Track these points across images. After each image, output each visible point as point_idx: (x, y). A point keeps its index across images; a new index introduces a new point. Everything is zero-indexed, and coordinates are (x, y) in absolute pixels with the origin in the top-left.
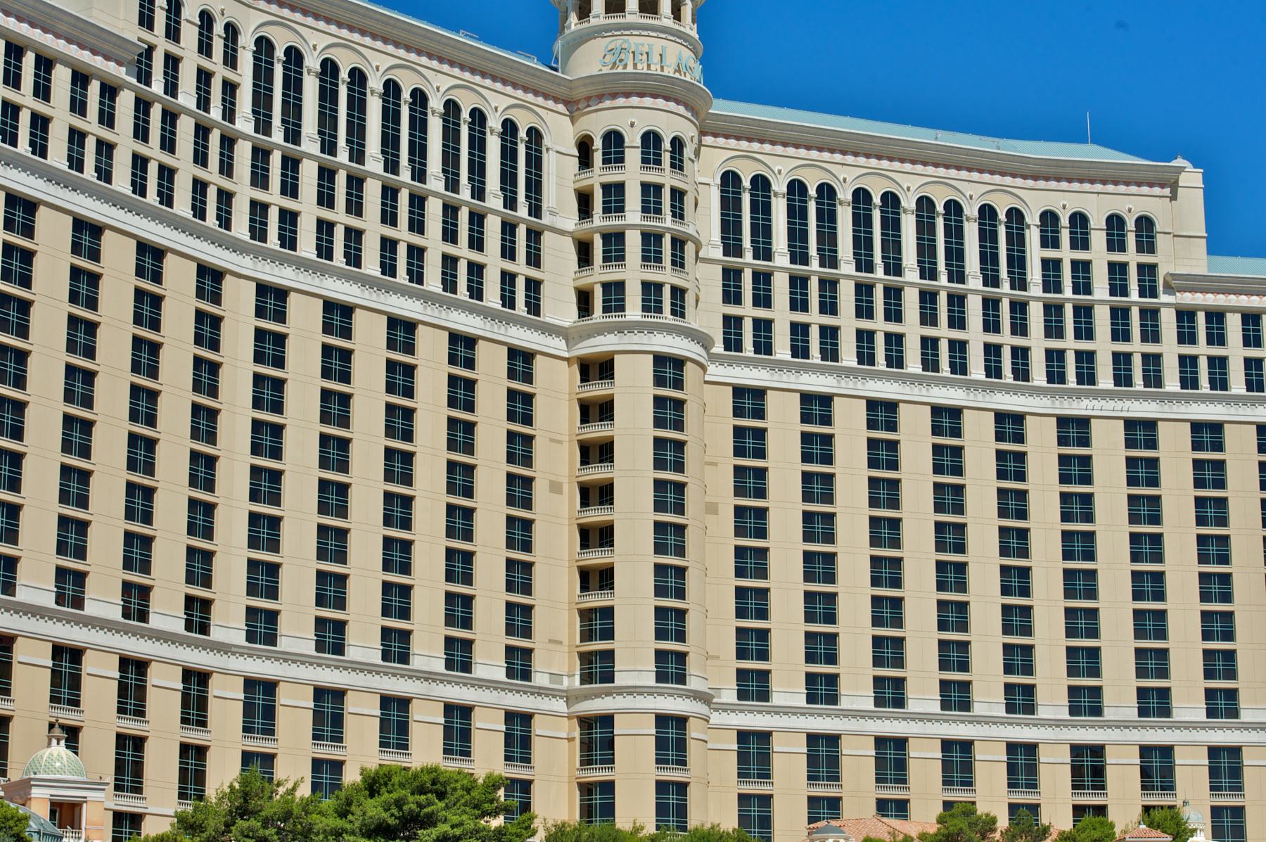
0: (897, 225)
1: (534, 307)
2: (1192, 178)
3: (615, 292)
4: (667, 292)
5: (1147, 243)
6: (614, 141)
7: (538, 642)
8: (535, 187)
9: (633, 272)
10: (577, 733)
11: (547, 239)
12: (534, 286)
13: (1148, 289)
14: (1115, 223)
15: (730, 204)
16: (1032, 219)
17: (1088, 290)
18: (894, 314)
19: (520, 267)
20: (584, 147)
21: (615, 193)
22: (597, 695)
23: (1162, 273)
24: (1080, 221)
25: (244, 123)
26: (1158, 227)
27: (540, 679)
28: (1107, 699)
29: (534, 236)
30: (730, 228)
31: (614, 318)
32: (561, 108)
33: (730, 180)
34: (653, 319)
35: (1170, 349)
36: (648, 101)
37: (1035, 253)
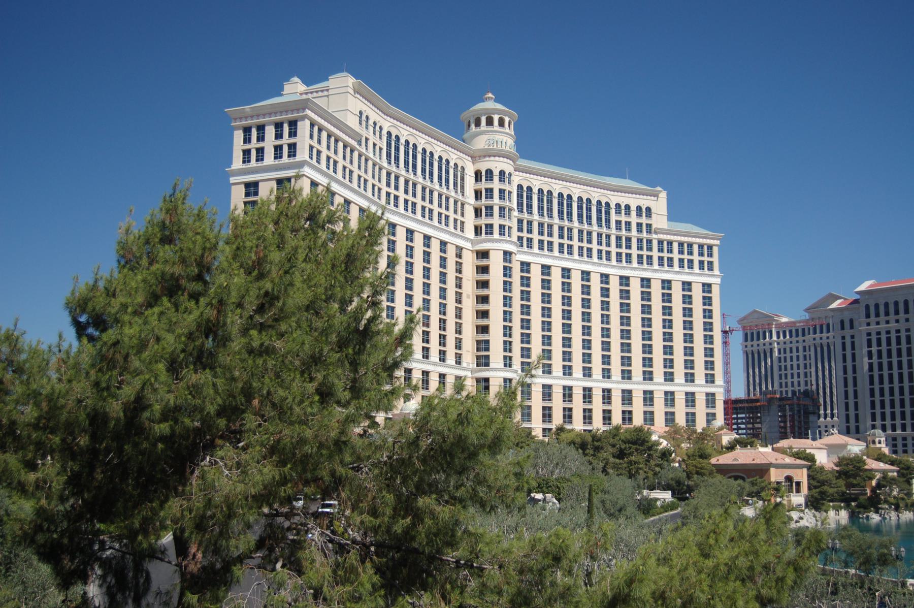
0: (590, 210)
1: (462, 231)
2: (663, 195)
3: (489, 227)
4: (507, 228)
6: (489, 172)
7: (463, 352)
8: (463, 187)
9: (496, 221)
11: (466, 206)
12: (462, 223)
14: (639, 209)
15: (520, 196)
16: (613, 206)
19: (459, 217)
21: (489, 192)
22: (484, 371)
23: (654, 227)
24: (628, 207)
27: (464, 364)
28: (633, 374)
30: (520, 205)
31: (489, 237)
32: (470, 159)
33: (520, 187)
34: (502, 238)
36: (501, 159)
37: (614, 217)
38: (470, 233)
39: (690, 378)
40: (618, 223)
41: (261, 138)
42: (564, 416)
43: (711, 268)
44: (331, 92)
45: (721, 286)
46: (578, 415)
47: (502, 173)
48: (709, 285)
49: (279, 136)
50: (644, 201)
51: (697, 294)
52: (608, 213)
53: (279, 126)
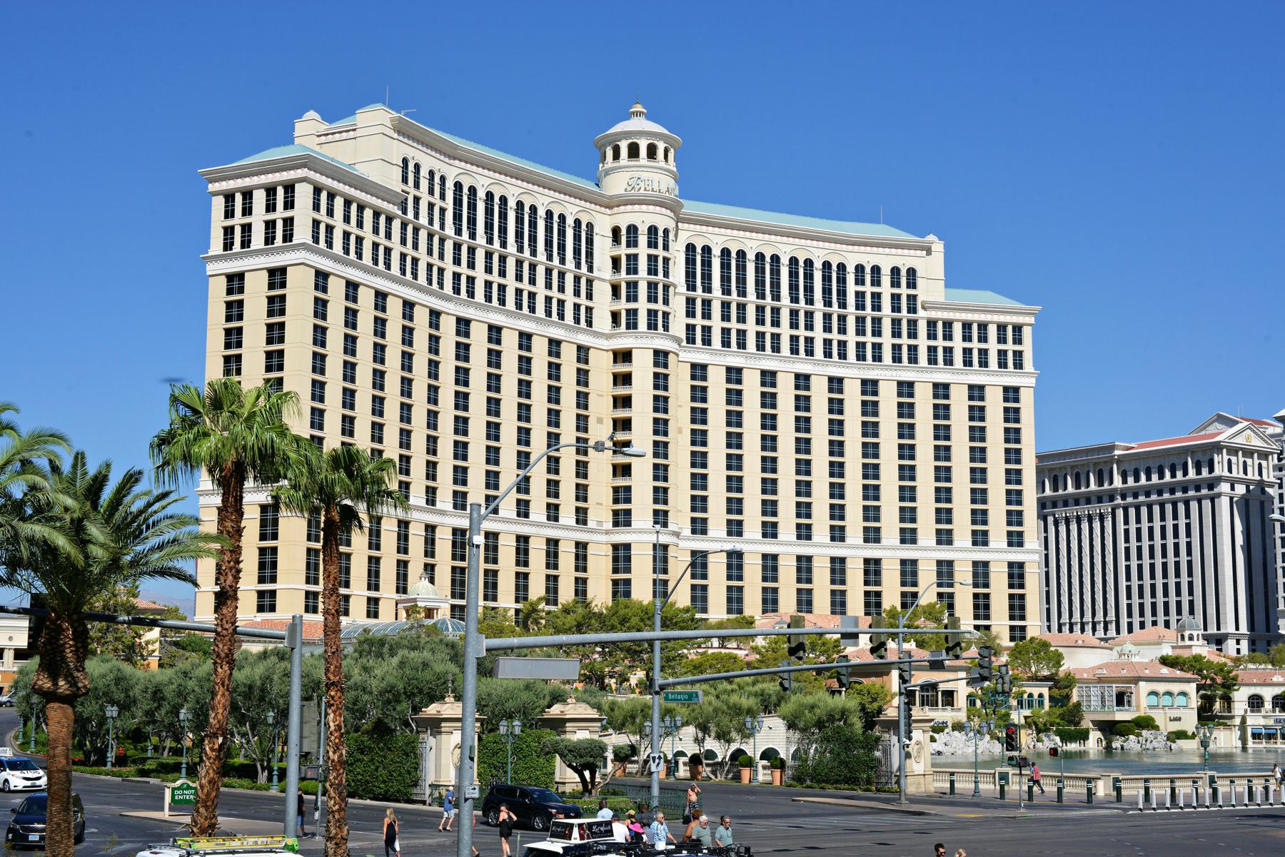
1: (589, 323)
2: (938, 247)
4: (660, 315)
5: (912, 284)
7: (591, 504)
8: (590, 254)
10: (610, 553)
11: (595, 284)
12: (589, 310)
13: (912, 309)
14: (895, 271)
15: (690, 262)
16: (851, 269)
17: (879, 309)
18: (776, 323)
19: (583, 301)
20: (616, 232)
24: (876, 270)
25: (450, 230)
26: (918, 274)
27: (591, 524)
29: (590, 282)
30: (690, 275)
33: (690, 248)
35: (923, 342)
37: (851, 288)
38: (602, 321)
39: (838, 534)
40: (860, 296)
41: (247, 211)
42: (799, 602)
43: (1019, 365)
44: (358, 133)
45: (1037, 390)
46: (822, 600)
47: (653, 230)
48: (1016, 390)
49: (271, 207)
50: (905, 260)
51: (994, 405)
52: (842, 281)
53: (271, 191)
